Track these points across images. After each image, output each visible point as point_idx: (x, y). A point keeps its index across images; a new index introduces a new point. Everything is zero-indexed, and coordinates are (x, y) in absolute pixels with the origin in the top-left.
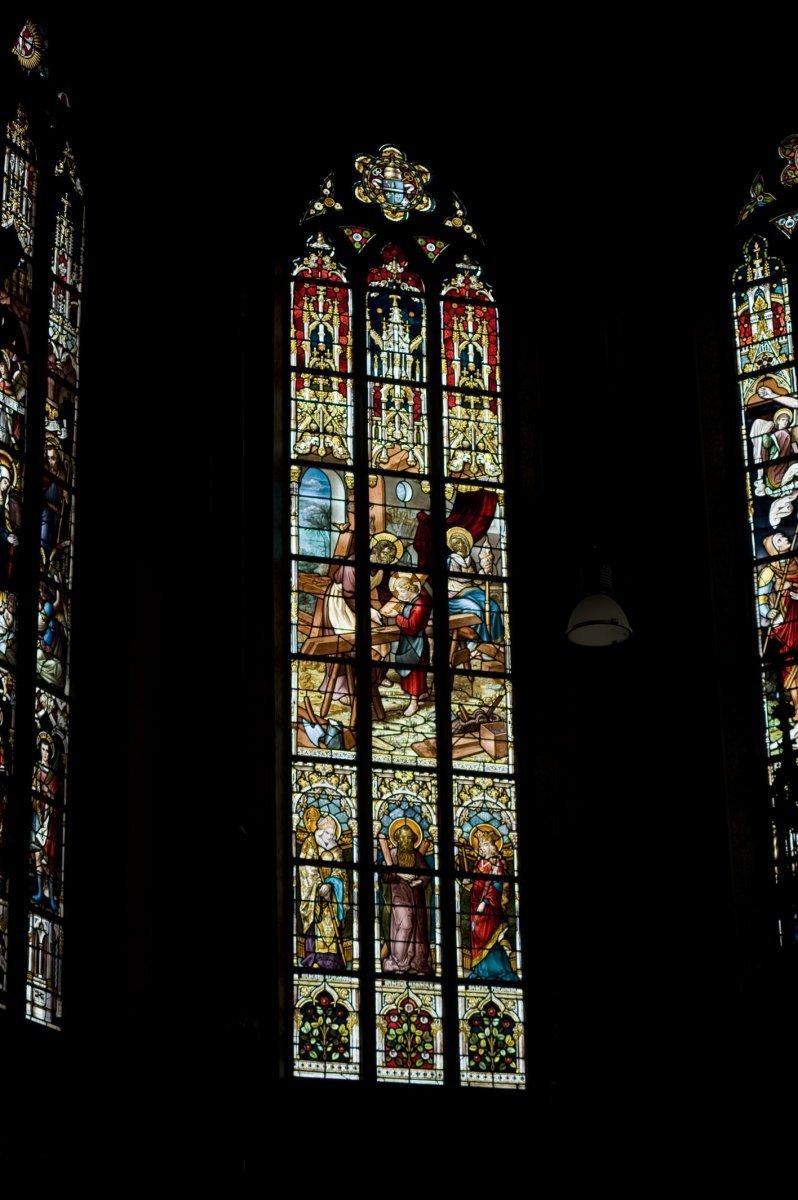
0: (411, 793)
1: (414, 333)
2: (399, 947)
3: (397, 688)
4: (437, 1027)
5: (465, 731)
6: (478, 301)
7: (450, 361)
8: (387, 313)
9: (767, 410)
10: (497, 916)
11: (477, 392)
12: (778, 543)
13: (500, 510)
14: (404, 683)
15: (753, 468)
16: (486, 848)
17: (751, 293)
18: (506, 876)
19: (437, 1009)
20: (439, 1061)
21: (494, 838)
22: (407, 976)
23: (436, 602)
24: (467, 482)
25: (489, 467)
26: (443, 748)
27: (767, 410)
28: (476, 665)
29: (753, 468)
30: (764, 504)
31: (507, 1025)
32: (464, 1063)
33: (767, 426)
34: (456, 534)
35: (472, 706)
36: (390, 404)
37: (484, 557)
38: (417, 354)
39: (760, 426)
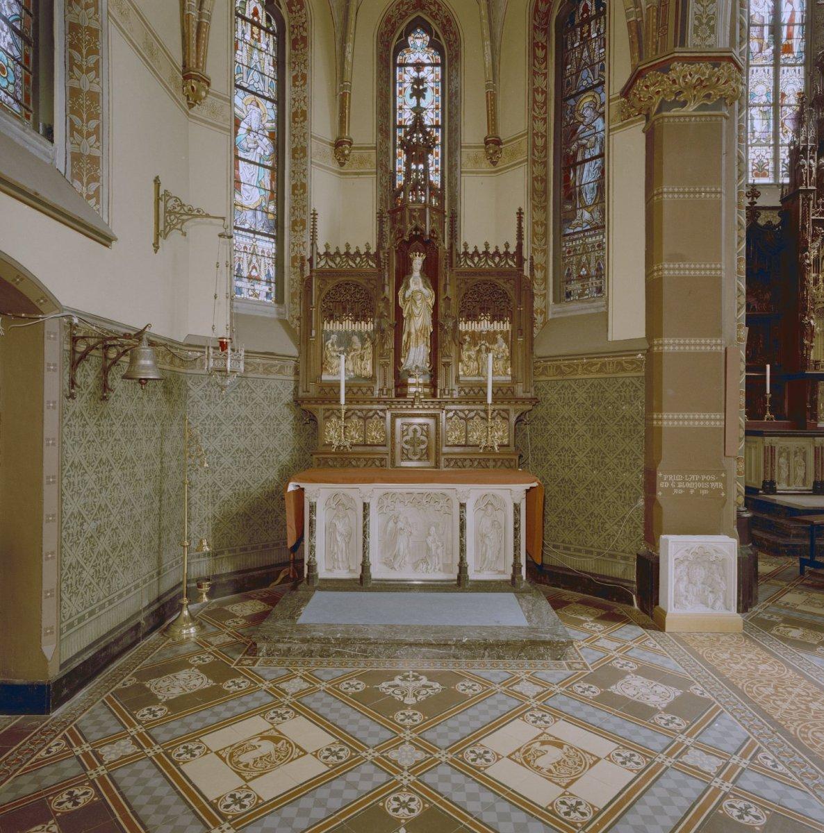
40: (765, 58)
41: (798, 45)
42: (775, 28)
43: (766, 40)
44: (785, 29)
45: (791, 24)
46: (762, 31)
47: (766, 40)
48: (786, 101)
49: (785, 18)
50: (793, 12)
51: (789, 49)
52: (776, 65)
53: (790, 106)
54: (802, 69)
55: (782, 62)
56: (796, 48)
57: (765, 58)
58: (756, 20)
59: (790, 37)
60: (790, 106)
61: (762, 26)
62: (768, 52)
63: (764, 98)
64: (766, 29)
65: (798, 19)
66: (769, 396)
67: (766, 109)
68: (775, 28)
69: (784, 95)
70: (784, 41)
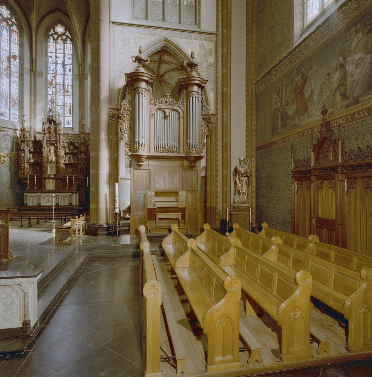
0: (6, 88)
1: (7, 33)
2: (4, 105)
3: (4, 76)
4: (8, 114)
5: (12, 82)
6: (16, 32)
7: (12, 38)
8: (4, 29)
9: (51, 57)
10: (15, 104)
11: (15, 43)
12: (51, 72)
13: (18, 58)
14: (5, 75)
15: (49, 63)
16: (15, 96)
17: (50, 43)
18: (17, 99)
19: (8, 112)
20: (8, 118)
21: (16, 95)
22: (5, 108)
23: (9, 67)
24: (14, 54)
25: (17, 53)
26: (10, 84)
27: (51, 57)
28: (14, 75)
29: (49, 63)
30: (50, 67)
31: (16, 115)
32: (11, 118)
33: (51, 59)
34: (12, 60)
35: (13, 80)
36: (4, 41)
37: (16, 63)
38: (8, 36)
39: (50, 58)
40: (61, 93)
41: (70, 90)
42: (64, 86)
43: (61, 89)
44: (66, 86)
45: (68, 85)
46: (60, 86)
47: (61, 89)
48: (67, 105)
49: (66, 83)
50: (69, 82)
51: (67, 91)
52: (64, 95)
53: (68, 106)
54: (71, 97)
55: (66, 95)
56: (70, 92)
57: (61, 93)
58: (58, 83)
59: (68, 88)
60: (68, 106)
61: (60, 85)
62: (62, 92)
63: (61, 104)
64: (61, 86)
65: (70, 84)
66: (35, 183)
67: (61, 107)
68: (64, 86)
69: (66, 103)
70: (66, 89)
